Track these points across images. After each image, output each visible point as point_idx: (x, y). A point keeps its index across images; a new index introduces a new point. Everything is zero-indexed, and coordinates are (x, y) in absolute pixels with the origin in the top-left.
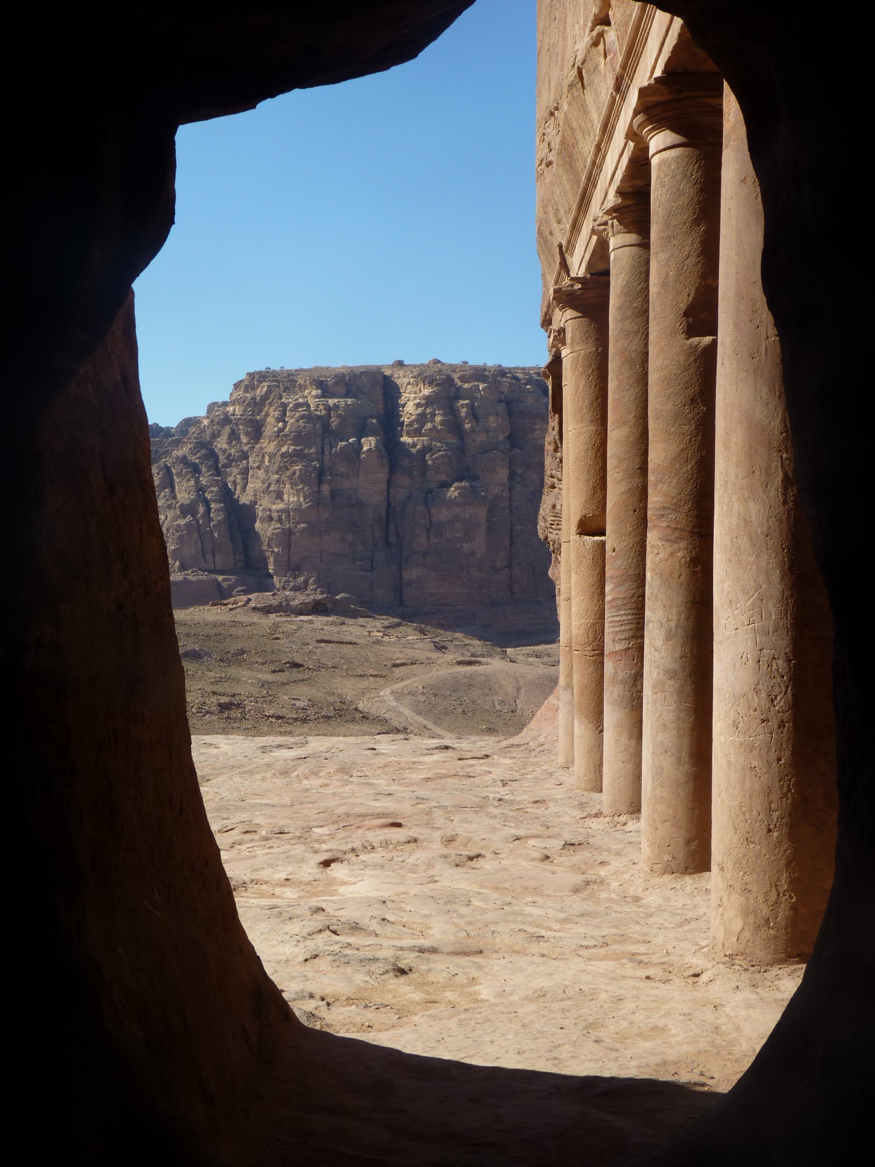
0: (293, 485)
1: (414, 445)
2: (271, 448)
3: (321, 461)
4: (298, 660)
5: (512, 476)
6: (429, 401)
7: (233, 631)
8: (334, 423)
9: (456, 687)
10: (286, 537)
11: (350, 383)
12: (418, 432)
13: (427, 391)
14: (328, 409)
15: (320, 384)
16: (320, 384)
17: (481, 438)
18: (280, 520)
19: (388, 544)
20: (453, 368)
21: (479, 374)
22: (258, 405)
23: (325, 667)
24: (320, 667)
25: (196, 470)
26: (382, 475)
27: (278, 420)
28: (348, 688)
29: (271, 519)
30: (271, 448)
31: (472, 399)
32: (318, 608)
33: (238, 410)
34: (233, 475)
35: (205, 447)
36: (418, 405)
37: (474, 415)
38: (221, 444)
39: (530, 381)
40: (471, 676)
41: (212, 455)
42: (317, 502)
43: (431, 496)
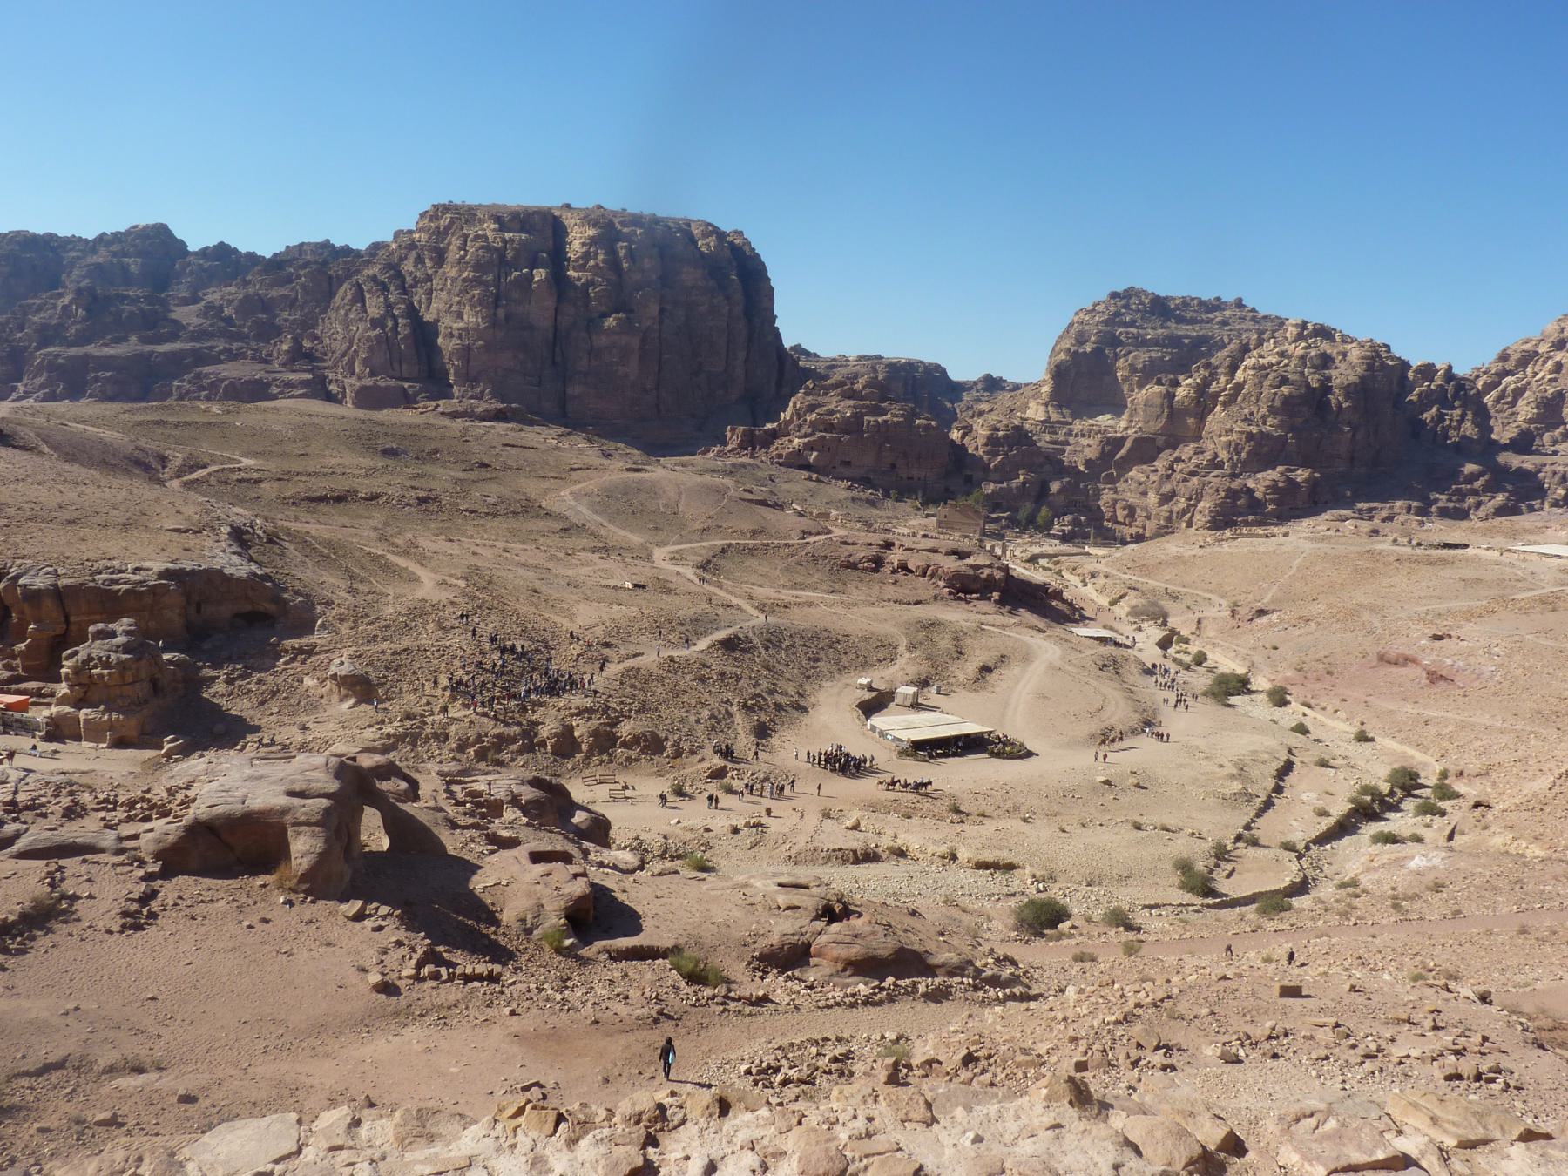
0: (473, 306)
1: (579, 279)
2: (453, 273)
3: (497, 286)
4: (486, 461)
5: (662, 311)
6: (593, 241)
7: (426, 432)
8: (510, 254)
9: (626, 490)
10: (465, 352)
11: (523, 220)
12: (582, 268)
13: (591, 232)
14: (505, 242)
15: (497, 219)
16: (497, 219)
17: (637, 277)
18: (460, 337)
19: (554, 363)
20: (615, 214)
21: (636, 220)
22: (441, 234)
23: (511, 468)
24: (506, 468)
25: (384, 288)
26: (550, 303)
27: (460, 249)
28: (531, 488)
29: (452, 335)
30: (453, 273)
31: (631, 242)
32: (499, 416)
33: (424, 237)
34: (419, 295)
35: (394, 268)
36: (583, 244)
37: (631, 255)
38: (408, 266)
39: (680, 230)
40: (639, 482)
41: (399, 276)
42: (494, 323)
43: (593, 324)
